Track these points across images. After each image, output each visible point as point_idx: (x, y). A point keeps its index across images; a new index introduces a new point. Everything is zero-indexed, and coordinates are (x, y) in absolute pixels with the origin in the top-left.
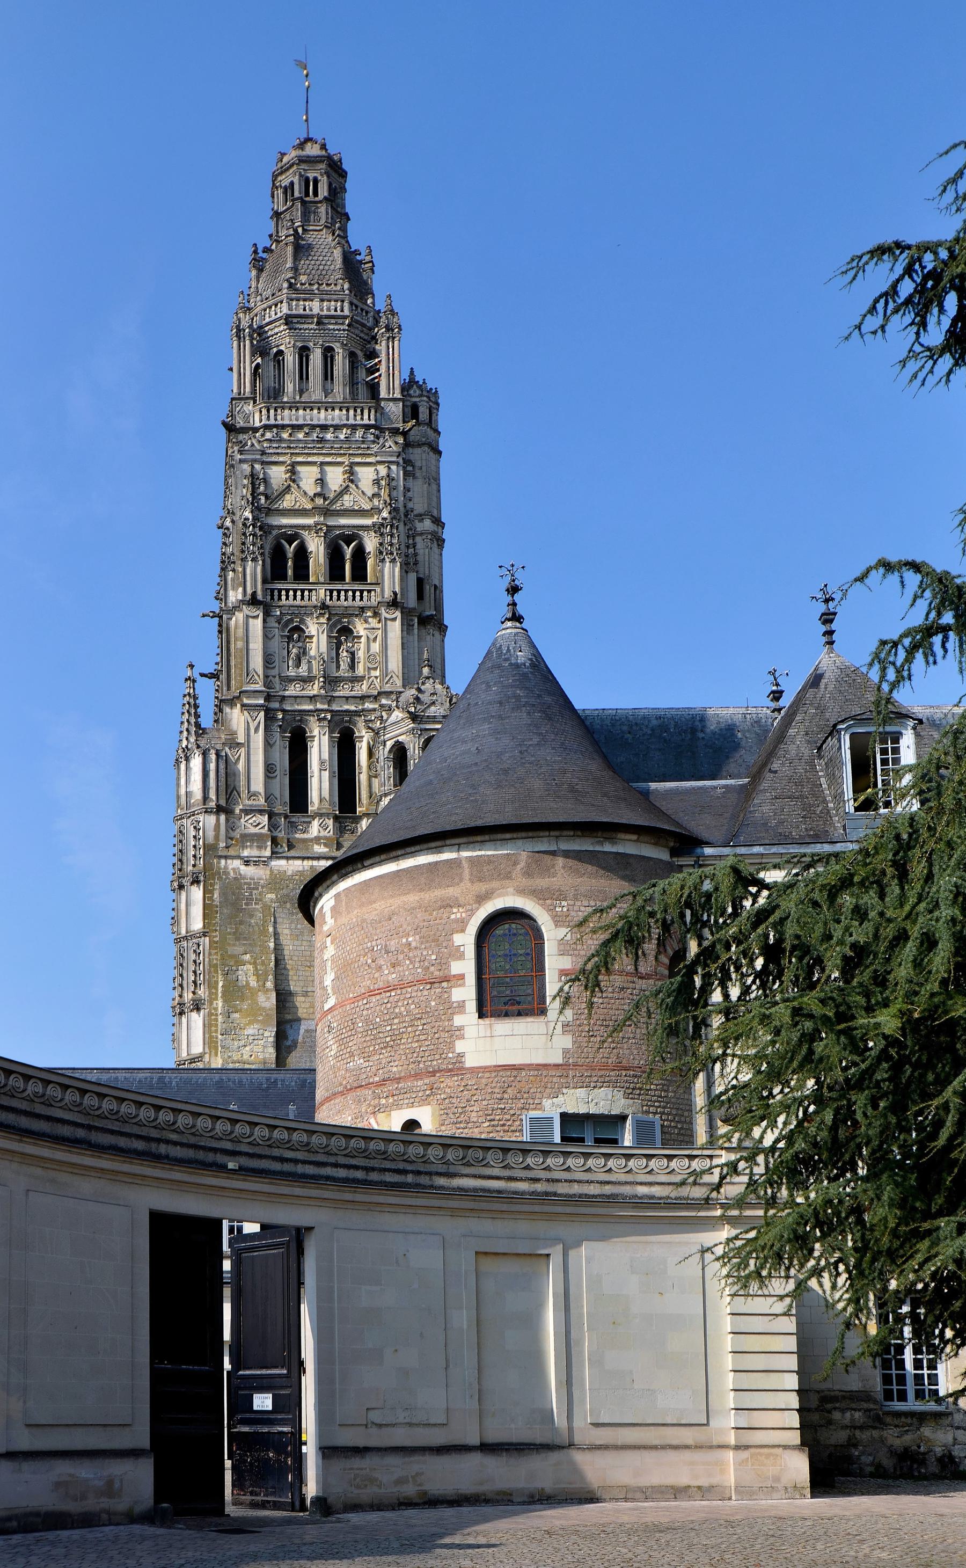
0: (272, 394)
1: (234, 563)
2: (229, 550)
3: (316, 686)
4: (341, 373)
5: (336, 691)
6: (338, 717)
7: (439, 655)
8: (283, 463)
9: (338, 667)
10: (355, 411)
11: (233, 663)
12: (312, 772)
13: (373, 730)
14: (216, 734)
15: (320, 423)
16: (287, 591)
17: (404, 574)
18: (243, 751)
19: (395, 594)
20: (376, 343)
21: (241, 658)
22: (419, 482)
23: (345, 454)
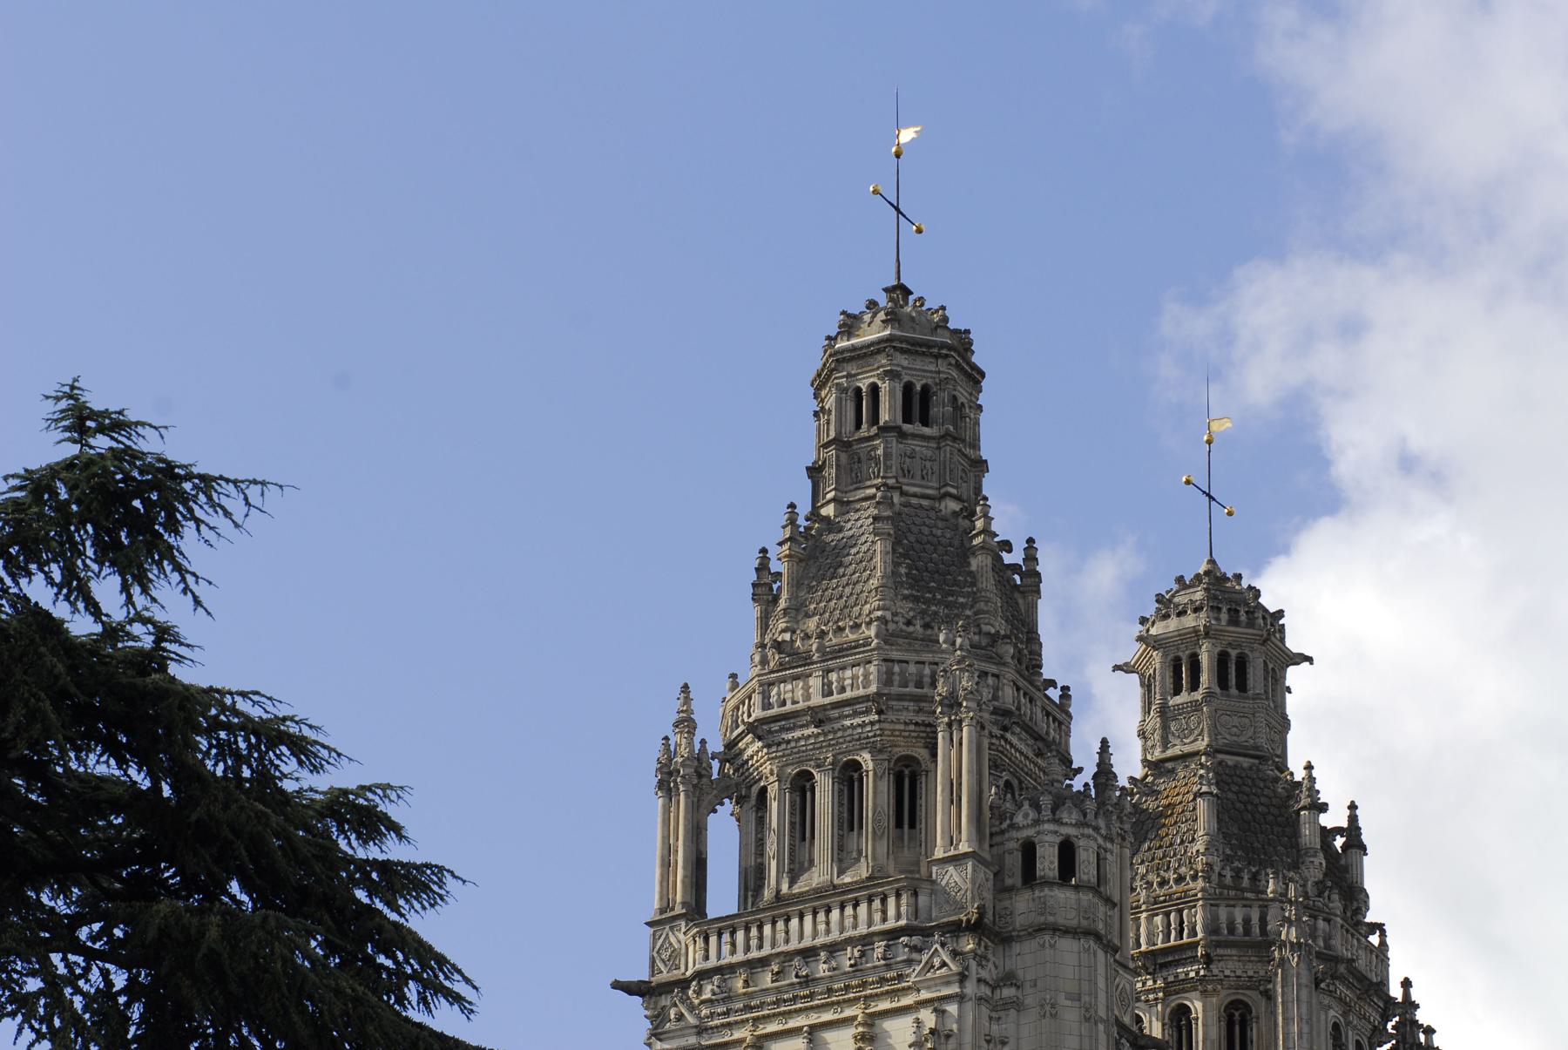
23: (857, 999)
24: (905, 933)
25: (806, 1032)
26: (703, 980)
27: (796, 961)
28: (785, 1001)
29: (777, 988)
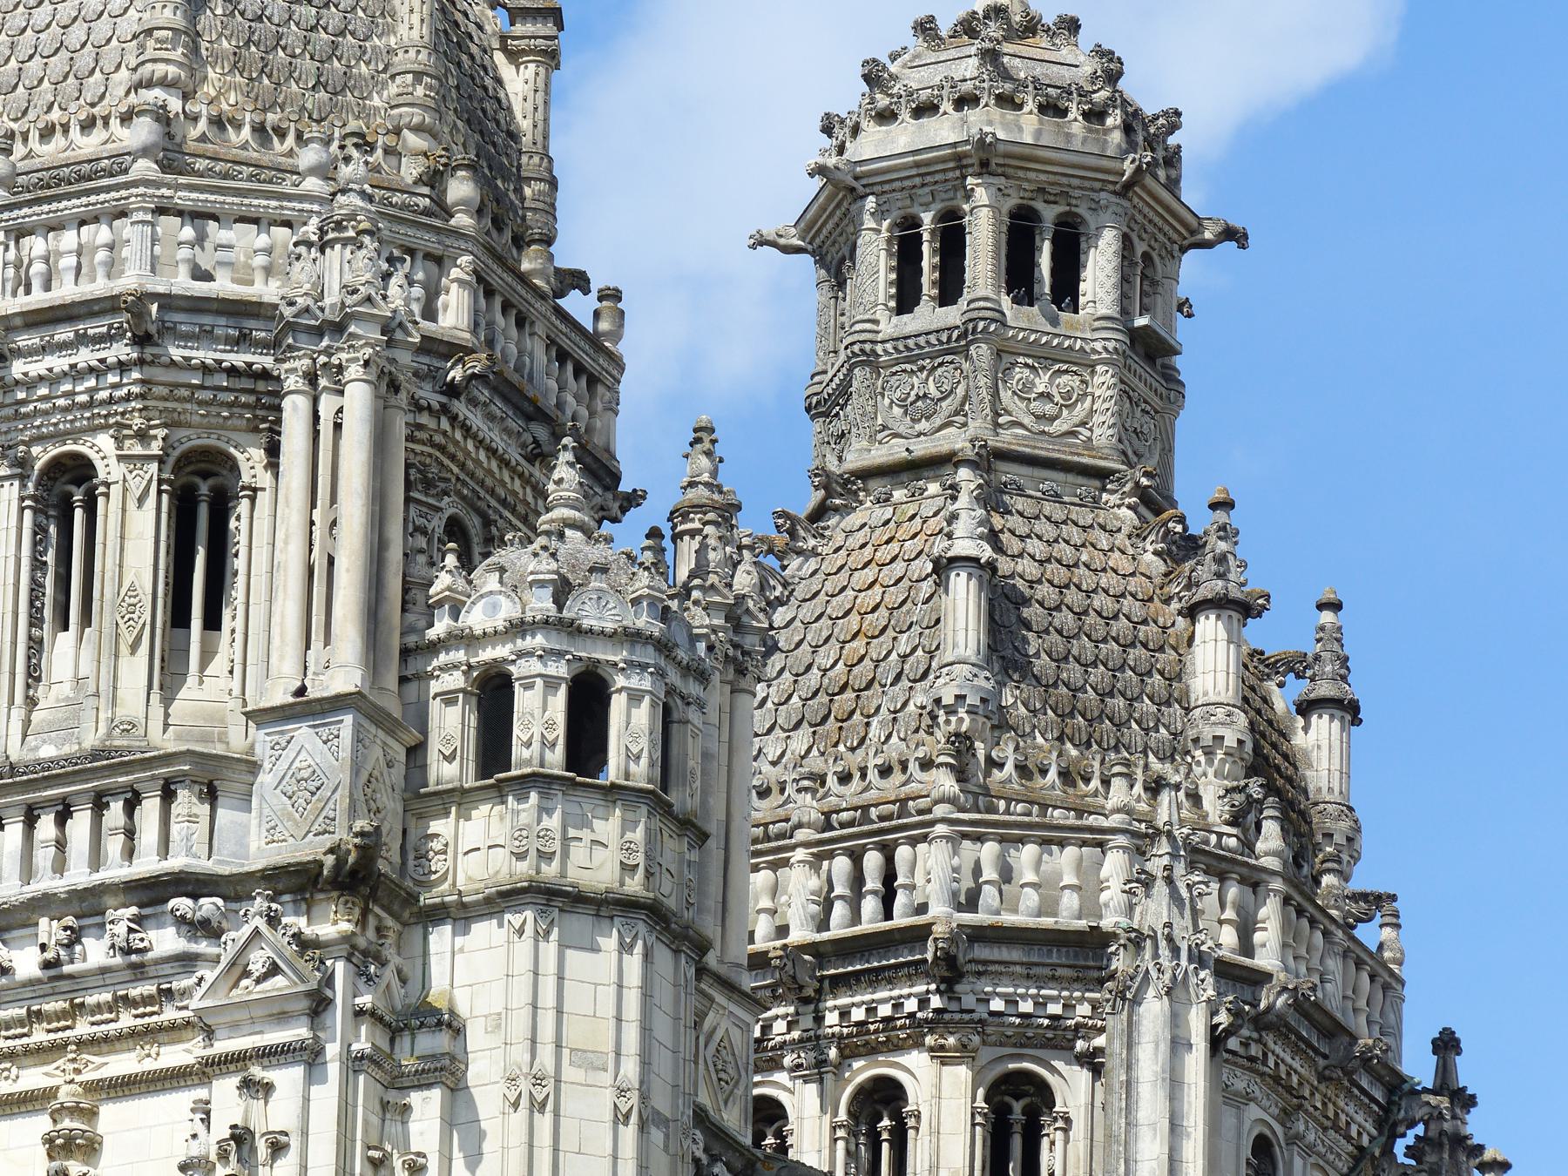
23: (58, 1048)
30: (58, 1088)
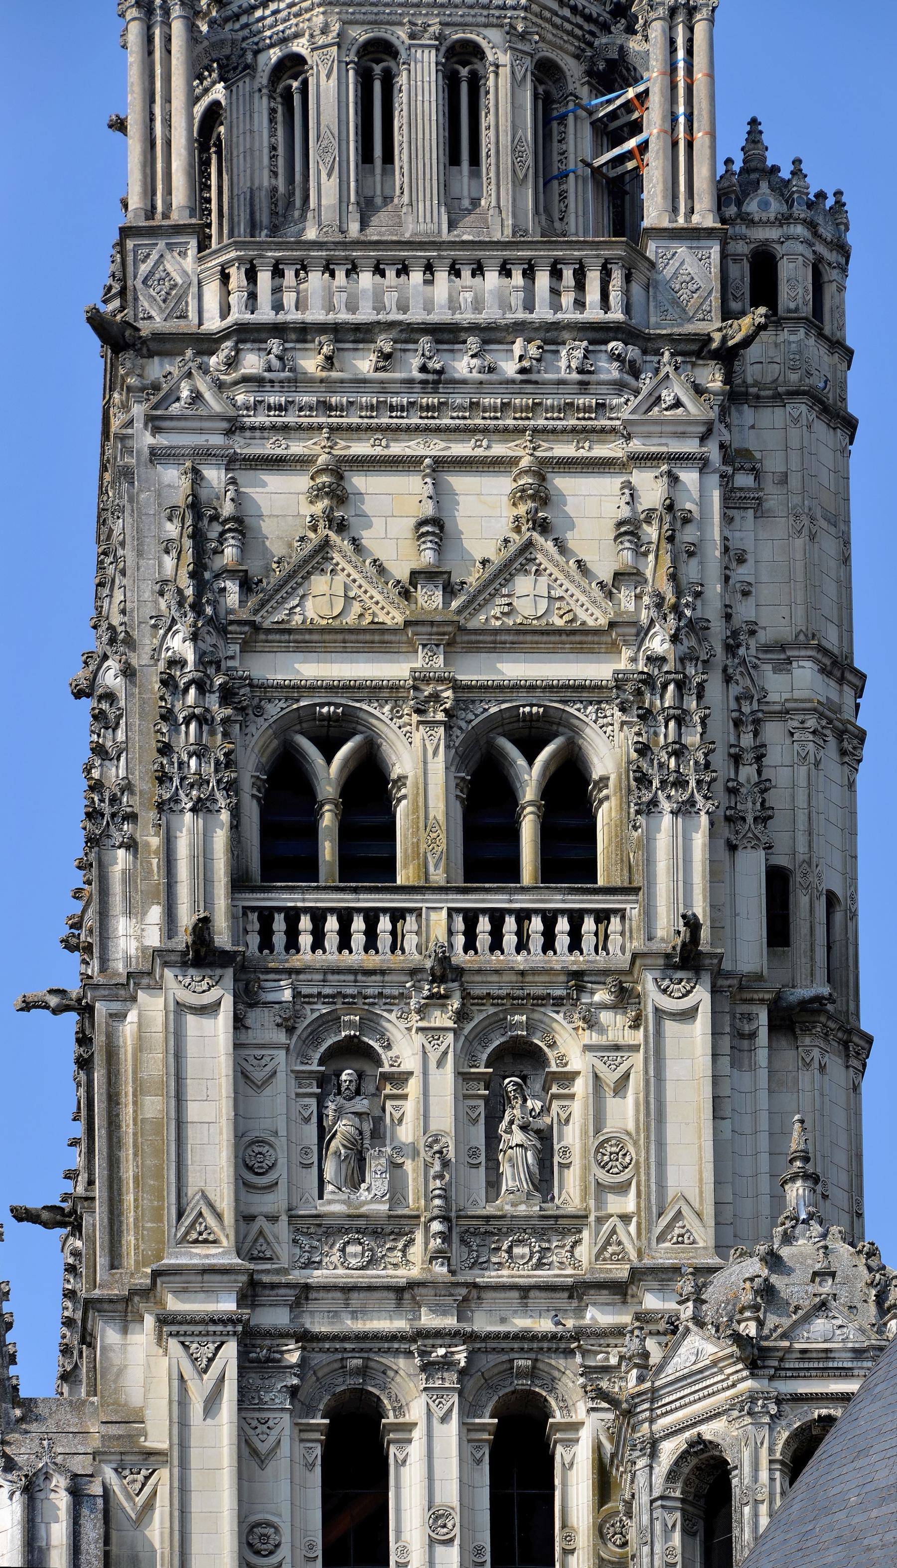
0: (264, 217)
1: (132, 817)
2: (115, 773)
3: (417, 1252)
4: (505, 140)
5: (484, 1266)
6: (493, 1359)
7: (843, 1141)
8: (301, 462)
9: (494, 1183)
10: (556, 274)
11: (128, 1172)
12: (404, 1550)
13: (614, 1402)
14: (69, 1419)
15: (434, 318)
16: (318, 917)
17: (723, 853)
18: (163, 1477)
19: (692, 924)
20: (631, 30)
21: (158, 1152)
22: (779, 527)
23: (519, 431)
24: (620, 336)
25: (428, 466)
26: (244, 341)
27: (425, 342)
28: (392, 408)
29: (382, 382)
30: (521, 458)
